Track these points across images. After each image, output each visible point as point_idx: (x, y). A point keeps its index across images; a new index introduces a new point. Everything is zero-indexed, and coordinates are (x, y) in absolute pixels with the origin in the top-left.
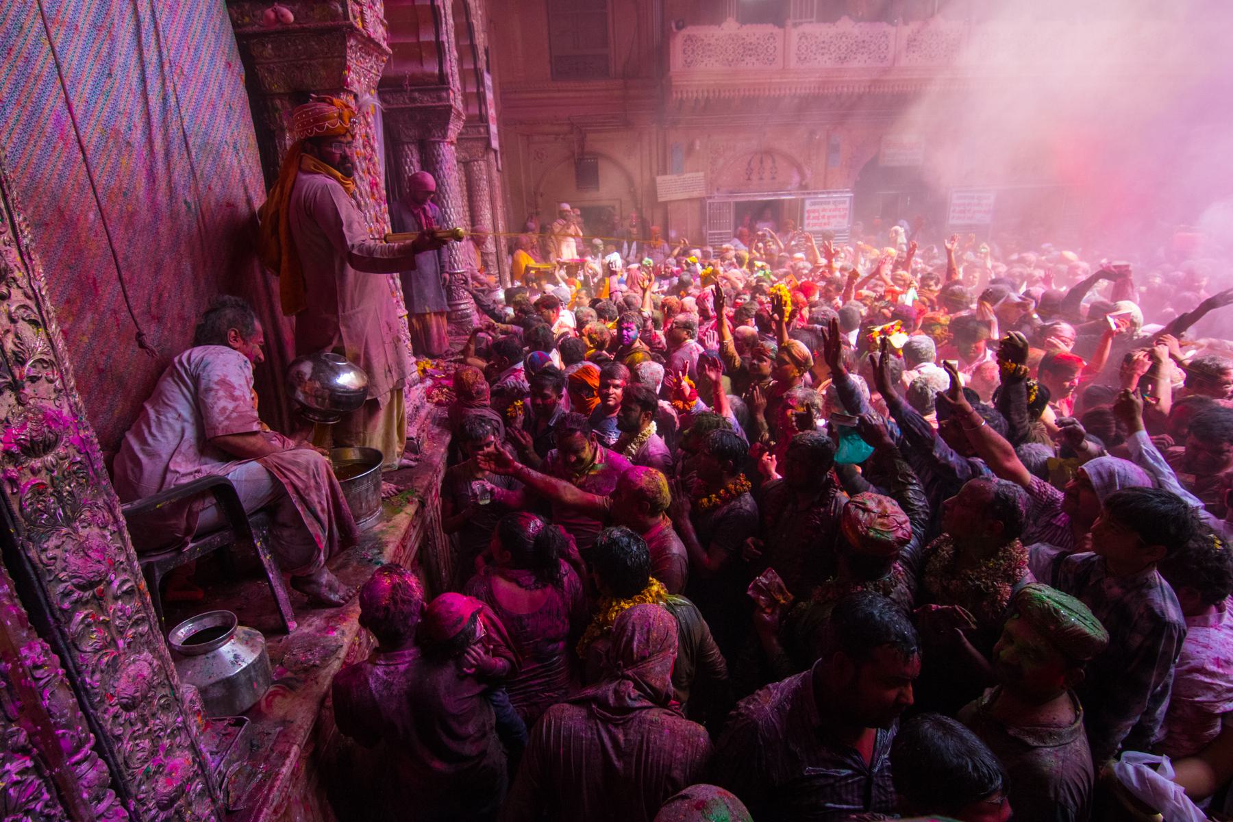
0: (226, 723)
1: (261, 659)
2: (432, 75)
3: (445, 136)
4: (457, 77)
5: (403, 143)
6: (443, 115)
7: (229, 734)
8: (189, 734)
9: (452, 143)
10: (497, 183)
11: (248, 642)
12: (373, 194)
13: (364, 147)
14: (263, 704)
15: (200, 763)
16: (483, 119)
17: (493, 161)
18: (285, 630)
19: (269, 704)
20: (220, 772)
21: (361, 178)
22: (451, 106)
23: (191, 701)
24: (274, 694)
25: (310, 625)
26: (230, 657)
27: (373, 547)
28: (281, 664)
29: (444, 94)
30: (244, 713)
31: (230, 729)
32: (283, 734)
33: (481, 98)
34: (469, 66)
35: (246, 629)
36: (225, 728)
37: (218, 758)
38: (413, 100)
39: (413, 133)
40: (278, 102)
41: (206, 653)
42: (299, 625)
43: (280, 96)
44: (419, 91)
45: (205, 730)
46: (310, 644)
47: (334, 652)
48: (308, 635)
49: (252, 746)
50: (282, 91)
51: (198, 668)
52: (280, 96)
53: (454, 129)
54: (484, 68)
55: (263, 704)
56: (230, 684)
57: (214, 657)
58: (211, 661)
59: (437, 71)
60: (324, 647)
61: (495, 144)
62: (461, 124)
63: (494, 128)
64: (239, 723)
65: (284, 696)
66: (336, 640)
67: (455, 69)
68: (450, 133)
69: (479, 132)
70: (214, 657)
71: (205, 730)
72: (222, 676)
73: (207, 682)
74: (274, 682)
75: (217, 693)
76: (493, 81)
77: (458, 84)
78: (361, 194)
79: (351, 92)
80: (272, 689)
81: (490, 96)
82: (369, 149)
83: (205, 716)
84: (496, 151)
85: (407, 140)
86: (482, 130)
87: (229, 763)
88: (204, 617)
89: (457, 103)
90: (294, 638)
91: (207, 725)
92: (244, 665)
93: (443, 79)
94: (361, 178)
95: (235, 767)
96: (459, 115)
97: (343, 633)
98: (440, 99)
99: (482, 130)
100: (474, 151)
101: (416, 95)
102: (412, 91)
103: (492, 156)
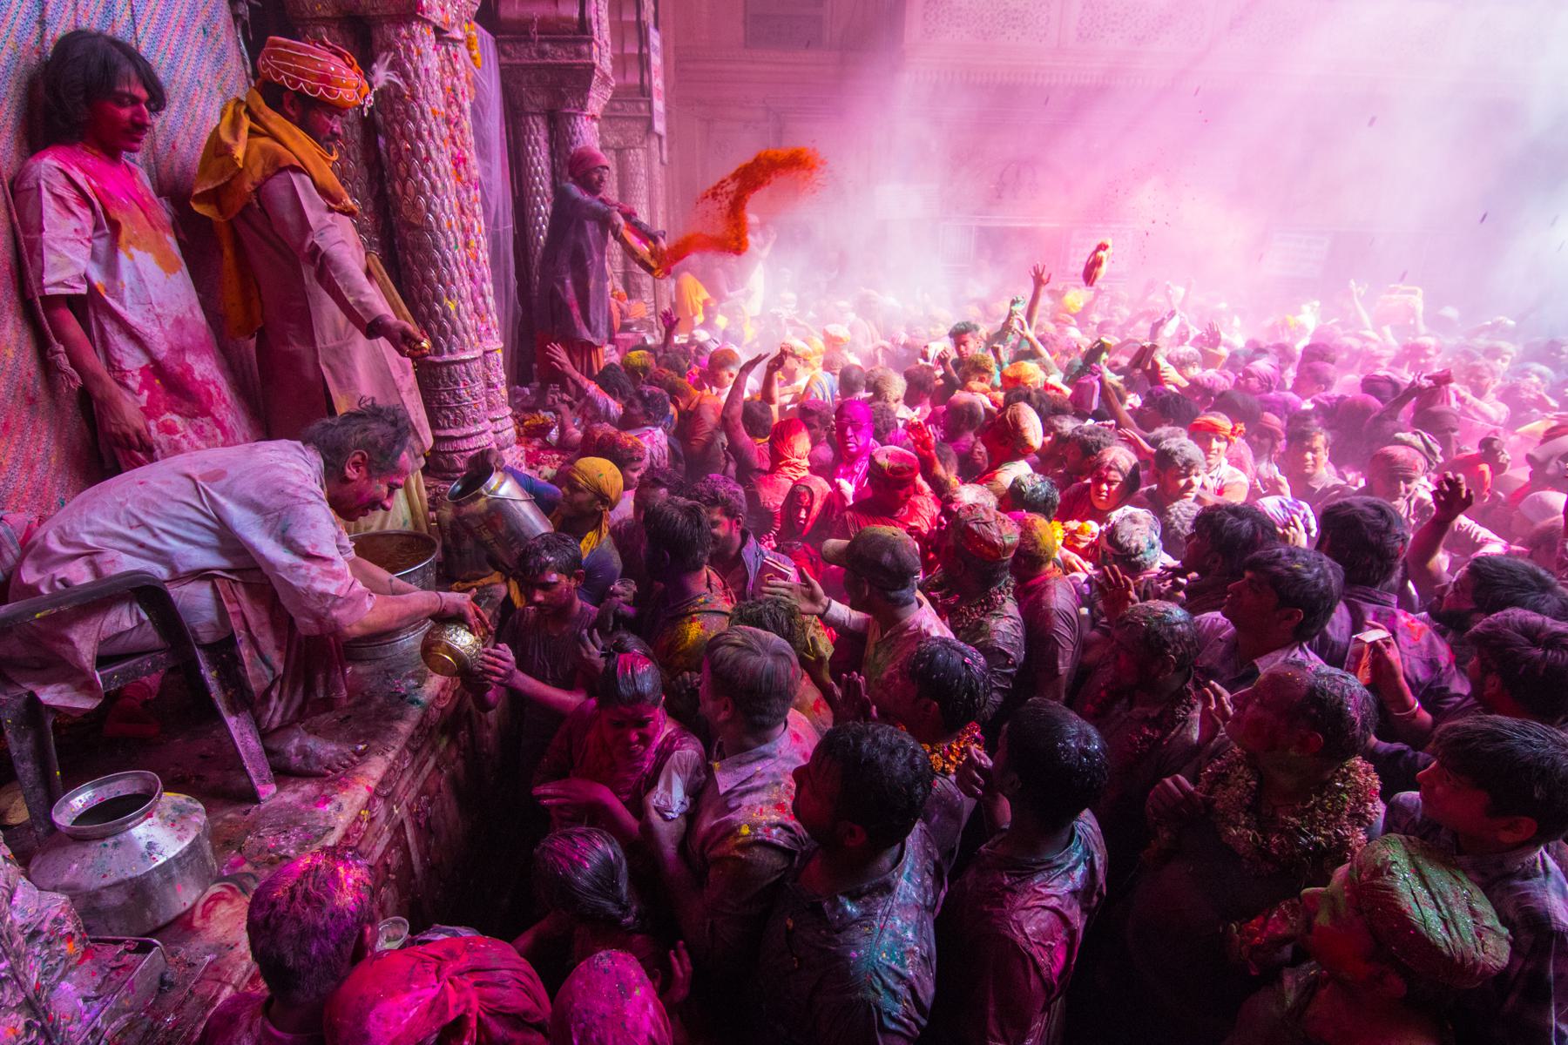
0: (122, 948)
1: (194, 848)
2: (569, 20)
3: (583, 107)
4: (606, 25)
5: (527, 114)
6: (582, 77)
7: (124, 967)
8: (21, 985)
9: (593, 117)
10: (659, 180)
11: (177, 821)
12: (459, 174)
13: (449, 105)
14: (198, 912)
15: (43, 1031)
16: (645, 91)
17: (655, 149)
18: (254, 798)
19: (206, 915)
20: (95, 1031)
21: (438, 148)
22: (593, 65)
23: (56, 920)
24: (217, 898)
25: (295, 791)
26: (143, 844)
27: (413, 676)
28: (240, 850)
29: (585, 48)
30: (156, 932)
31: (129, 958)
32: (214, 967)
33: (644, 62)
34: (629, 16)
35: (181, 798)
36: (118, 958)
37: (97, 1005)
38: (542, 54)
39: (541, 100)
40: (323, 30)
41: (103, 838)
42: (280, 789)
43: (325, 21)
44: (552, 41)
45: (80, 962)
46: (288, 822)
47: (319, 837)
48: (289, 806)
49: (163, 982)
50: (329, 14)
51: (89, 860)
52: (325, 21)
53: (597, 100)
54: (651, 21)
55: (198, 912)
56: (140, 890)
57: (116, 845)
58: (109, 850)
59: (576, 15)
60: (305, 829)
61: (660, 126)
62: (609, 94)
63: (659, 105)
64: (145, 948)
65: (230, 901)
66: (327, 818)
67: (604, 15)
68: (590, 102)
69: (639, 110)
70: (116, 845)
71: (80, 962)
72: (122, 876)
73: (97, 883)
74: (220, 879)
75: (114, 899)
76: (664, 42)
77: (606, 35)
78: (437, 171)
79: (429, 22)
80: (215, 889)
81: (656, 60)
82: (455, 108)
83: (83, 941)
84: (660, 137)
85: (533, 109)
86: (643, 106)
87: (113, 1016)
88: (117, 778)
89: (603, 57)
90: (268, 809)
91: (87, 953)
92: (162, 860)
93: (583, 28)
94: (438, 148)
95: (122, 1021)
96: (605, 80)
97: (340, 808)
98: (579, 54)
99: (643, 106)
100: (631, 134)
101: (547, 46)
102: (541, 40)
103: (654, 142)
